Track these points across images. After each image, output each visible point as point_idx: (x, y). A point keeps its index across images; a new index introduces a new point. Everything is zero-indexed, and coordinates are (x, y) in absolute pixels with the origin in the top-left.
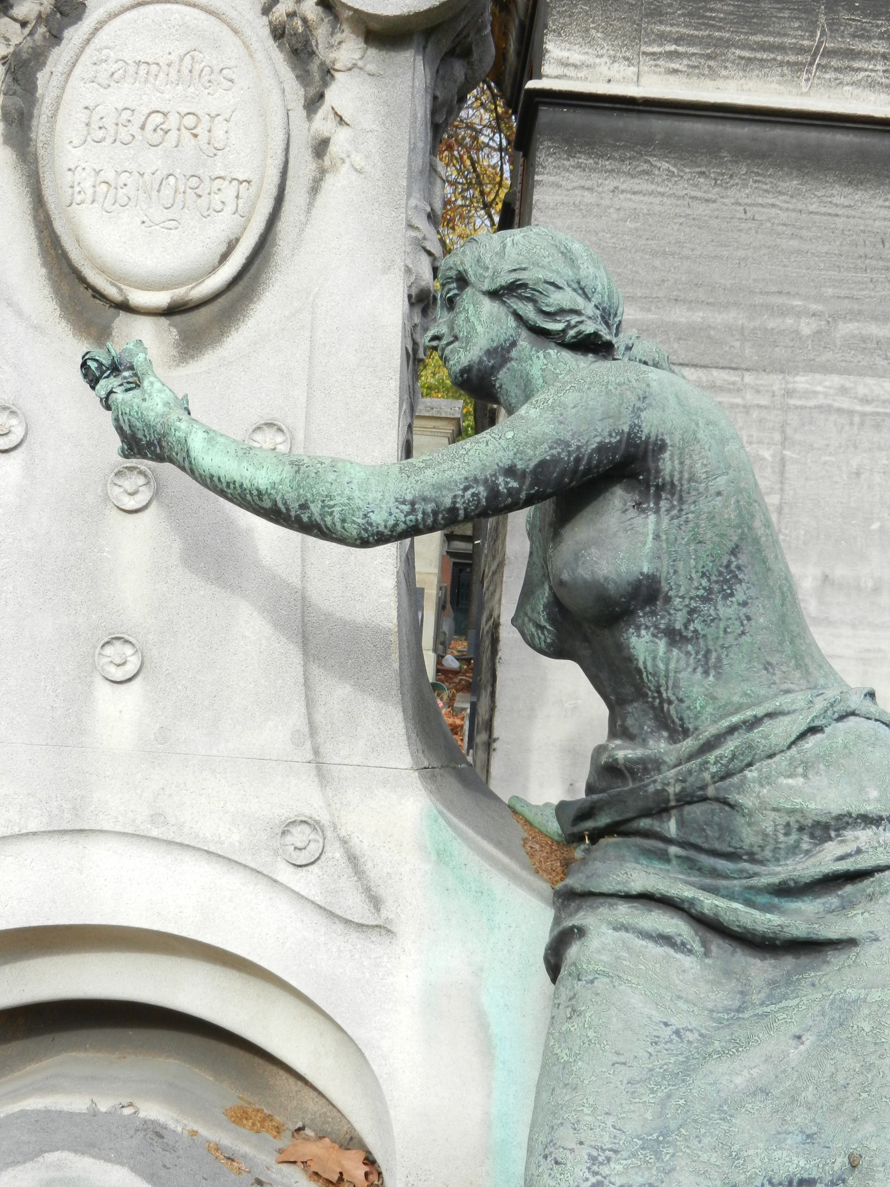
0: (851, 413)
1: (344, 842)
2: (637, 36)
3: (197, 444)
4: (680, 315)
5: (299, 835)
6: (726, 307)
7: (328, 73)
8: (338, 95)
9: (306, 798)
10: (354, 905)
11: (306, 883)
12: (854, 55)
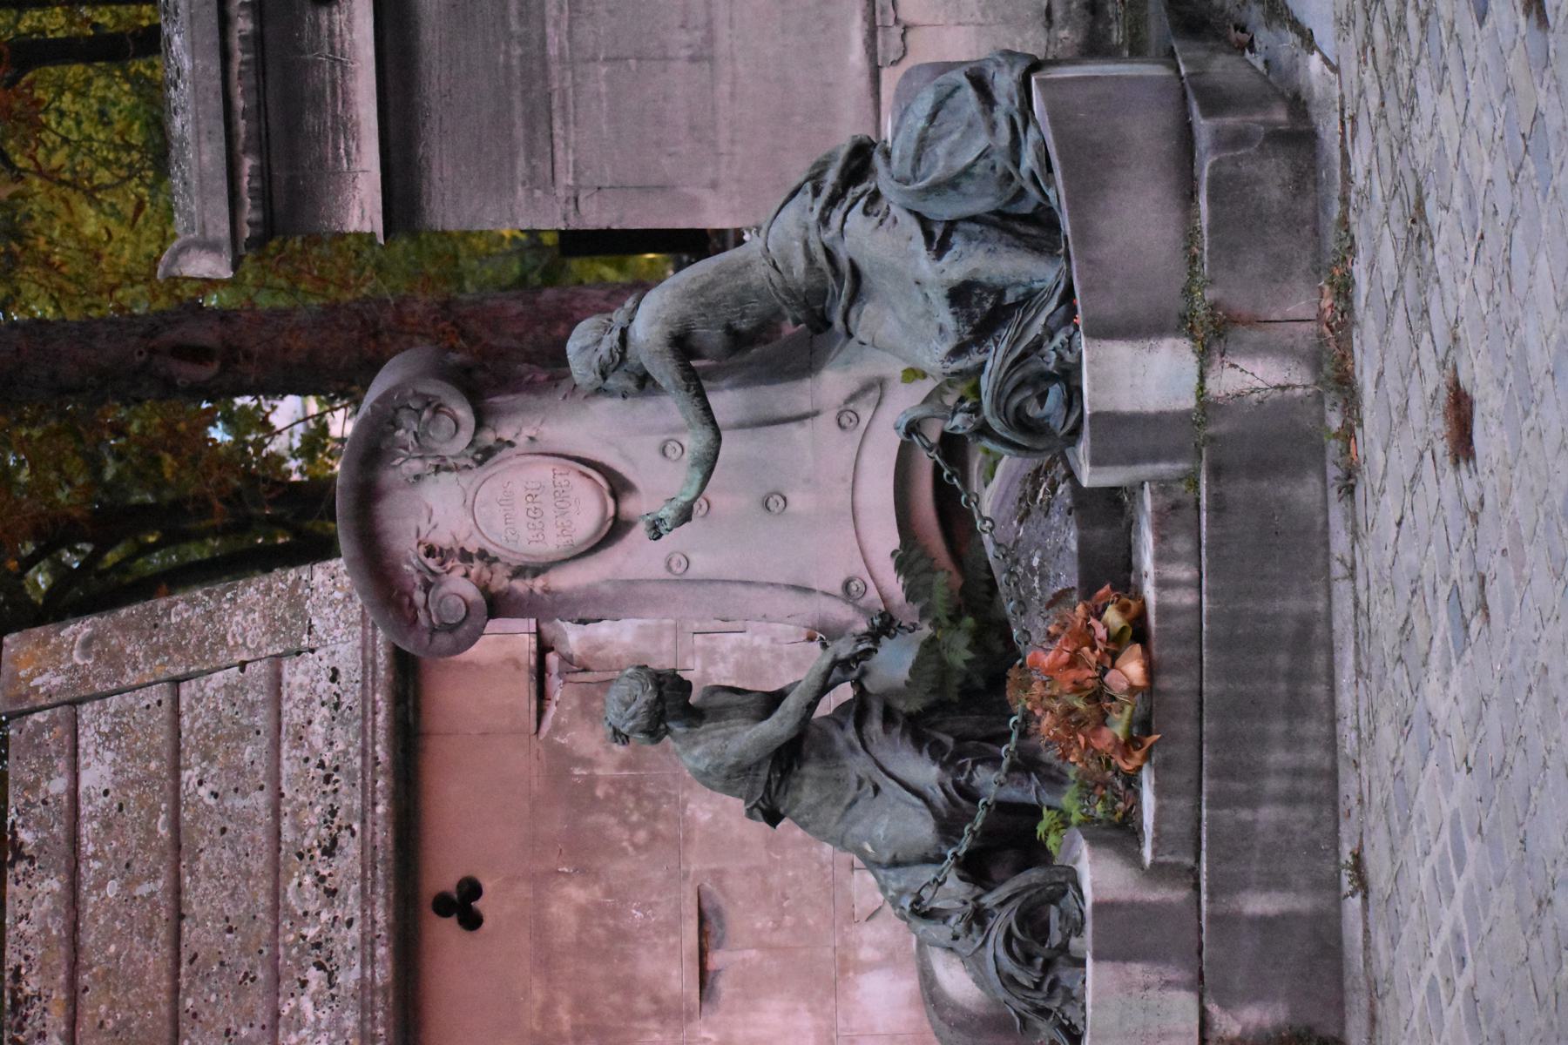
0: (571, 19)
1: (847, 402)
2: (338, 173)
3: (685, 498)
4: (519, 132)
5: (845, 421)
6: (510, 103)
7: (499, 440)
8: (507, 434)
9: (827, 421)
10: (873, 395)
11: (866, 415)
12: (331, 33)
